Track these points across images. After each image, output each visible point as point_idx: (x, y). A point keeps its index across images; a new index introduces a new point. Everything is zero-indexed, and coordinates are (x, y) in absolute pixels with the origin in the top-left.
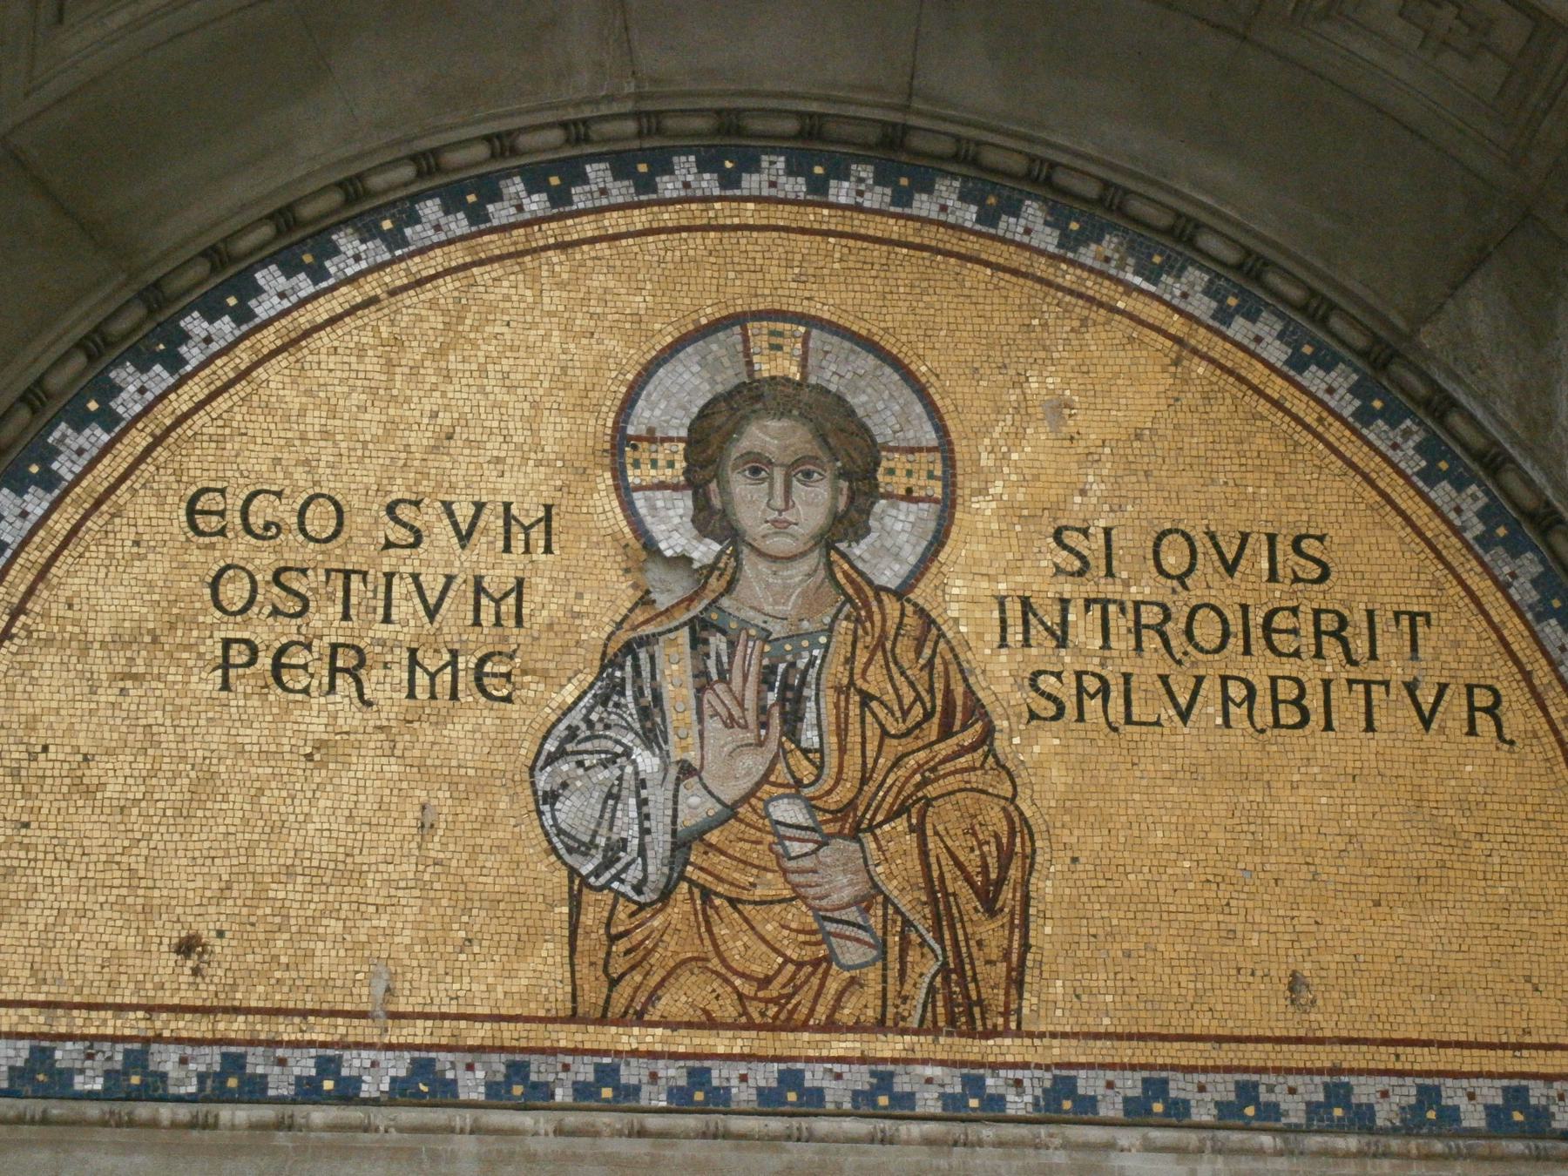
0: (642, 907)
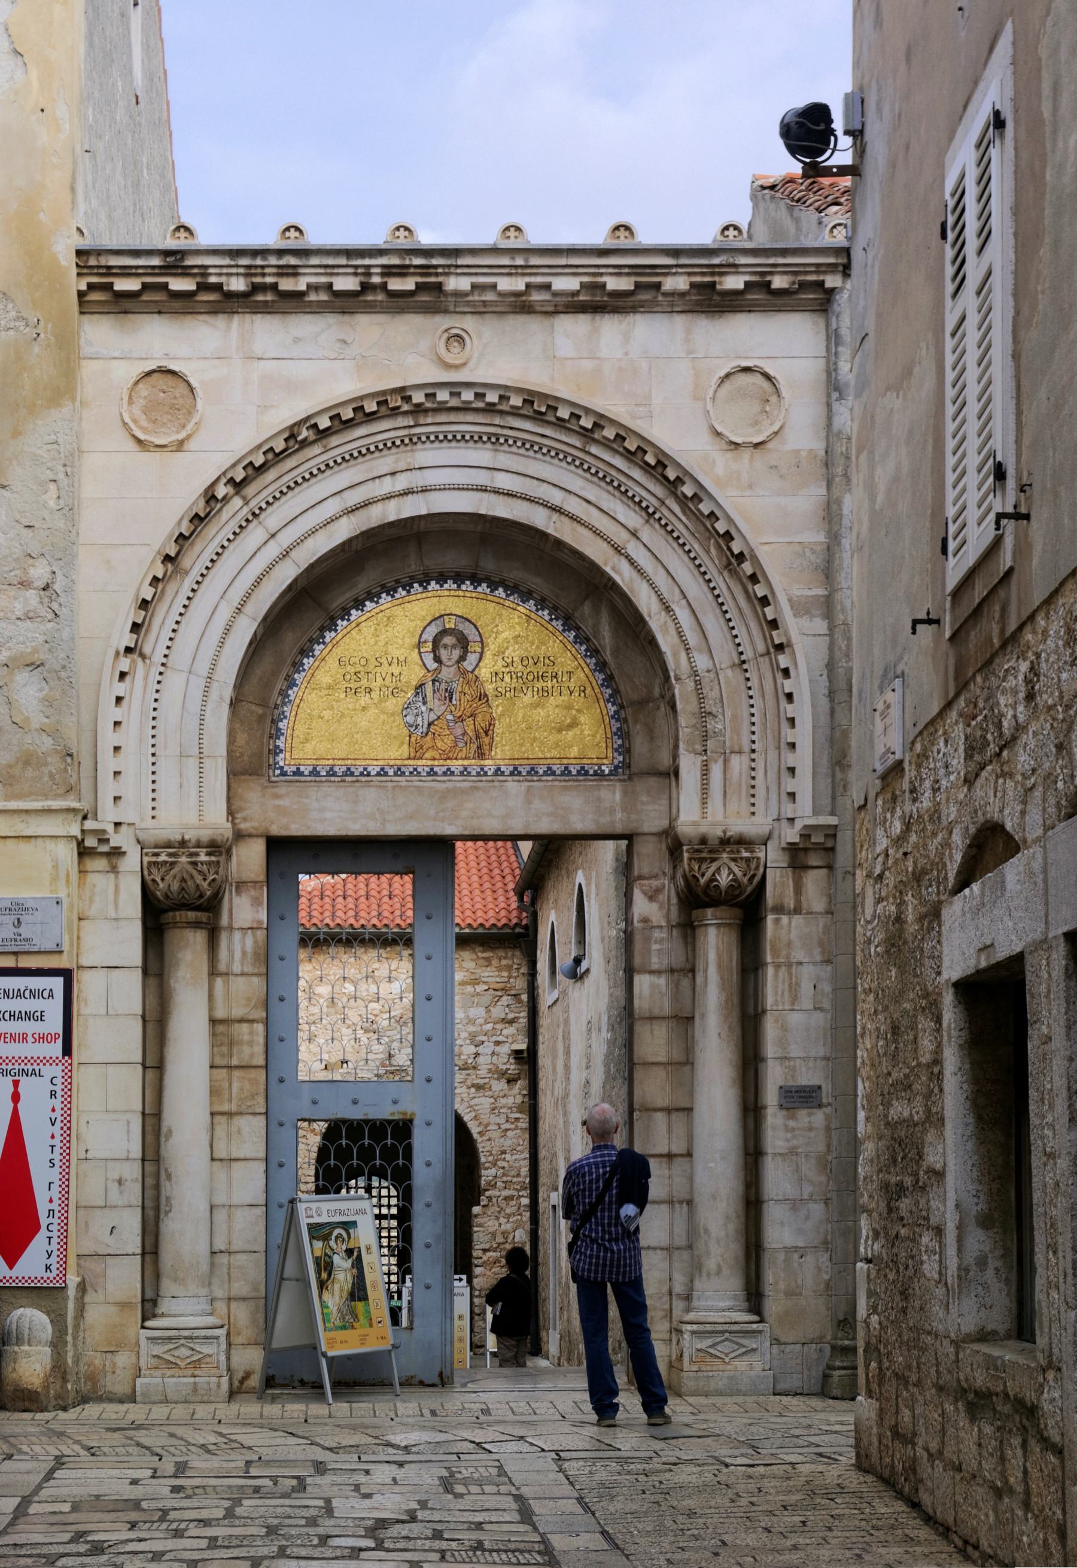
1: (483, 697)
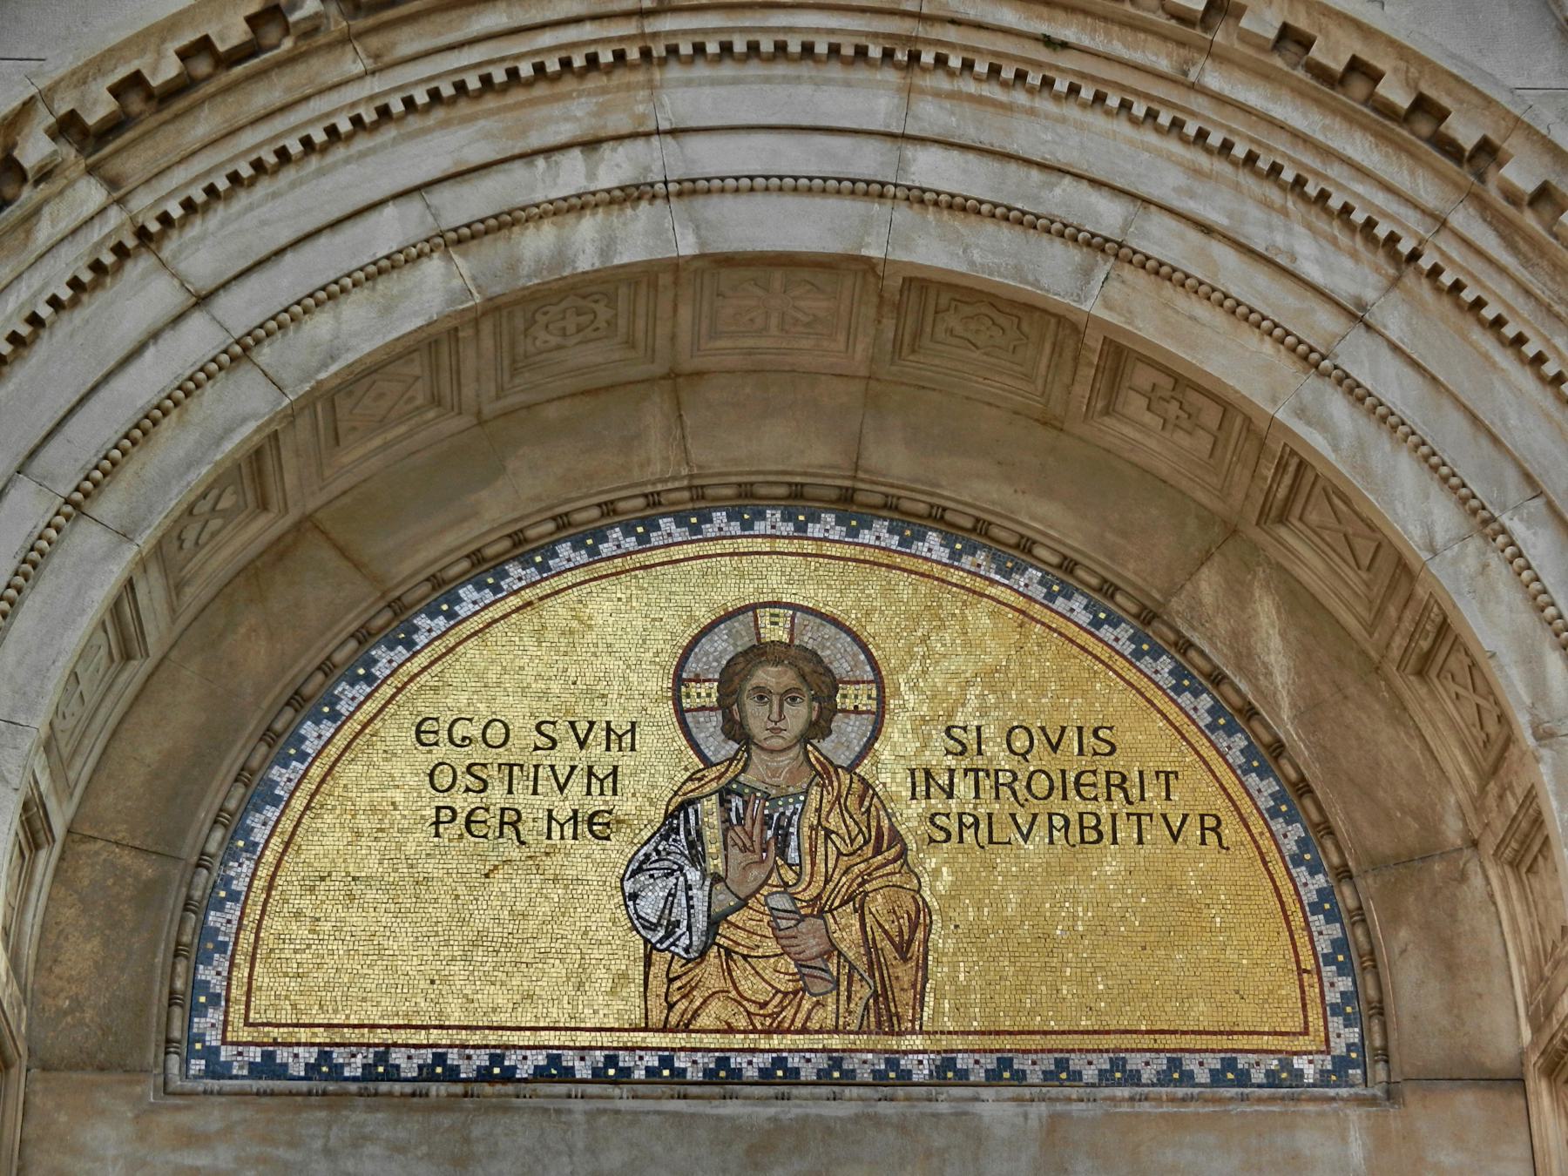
0: (689, 961)
1: (887, 842)
